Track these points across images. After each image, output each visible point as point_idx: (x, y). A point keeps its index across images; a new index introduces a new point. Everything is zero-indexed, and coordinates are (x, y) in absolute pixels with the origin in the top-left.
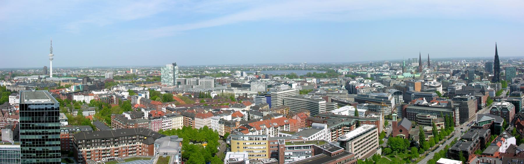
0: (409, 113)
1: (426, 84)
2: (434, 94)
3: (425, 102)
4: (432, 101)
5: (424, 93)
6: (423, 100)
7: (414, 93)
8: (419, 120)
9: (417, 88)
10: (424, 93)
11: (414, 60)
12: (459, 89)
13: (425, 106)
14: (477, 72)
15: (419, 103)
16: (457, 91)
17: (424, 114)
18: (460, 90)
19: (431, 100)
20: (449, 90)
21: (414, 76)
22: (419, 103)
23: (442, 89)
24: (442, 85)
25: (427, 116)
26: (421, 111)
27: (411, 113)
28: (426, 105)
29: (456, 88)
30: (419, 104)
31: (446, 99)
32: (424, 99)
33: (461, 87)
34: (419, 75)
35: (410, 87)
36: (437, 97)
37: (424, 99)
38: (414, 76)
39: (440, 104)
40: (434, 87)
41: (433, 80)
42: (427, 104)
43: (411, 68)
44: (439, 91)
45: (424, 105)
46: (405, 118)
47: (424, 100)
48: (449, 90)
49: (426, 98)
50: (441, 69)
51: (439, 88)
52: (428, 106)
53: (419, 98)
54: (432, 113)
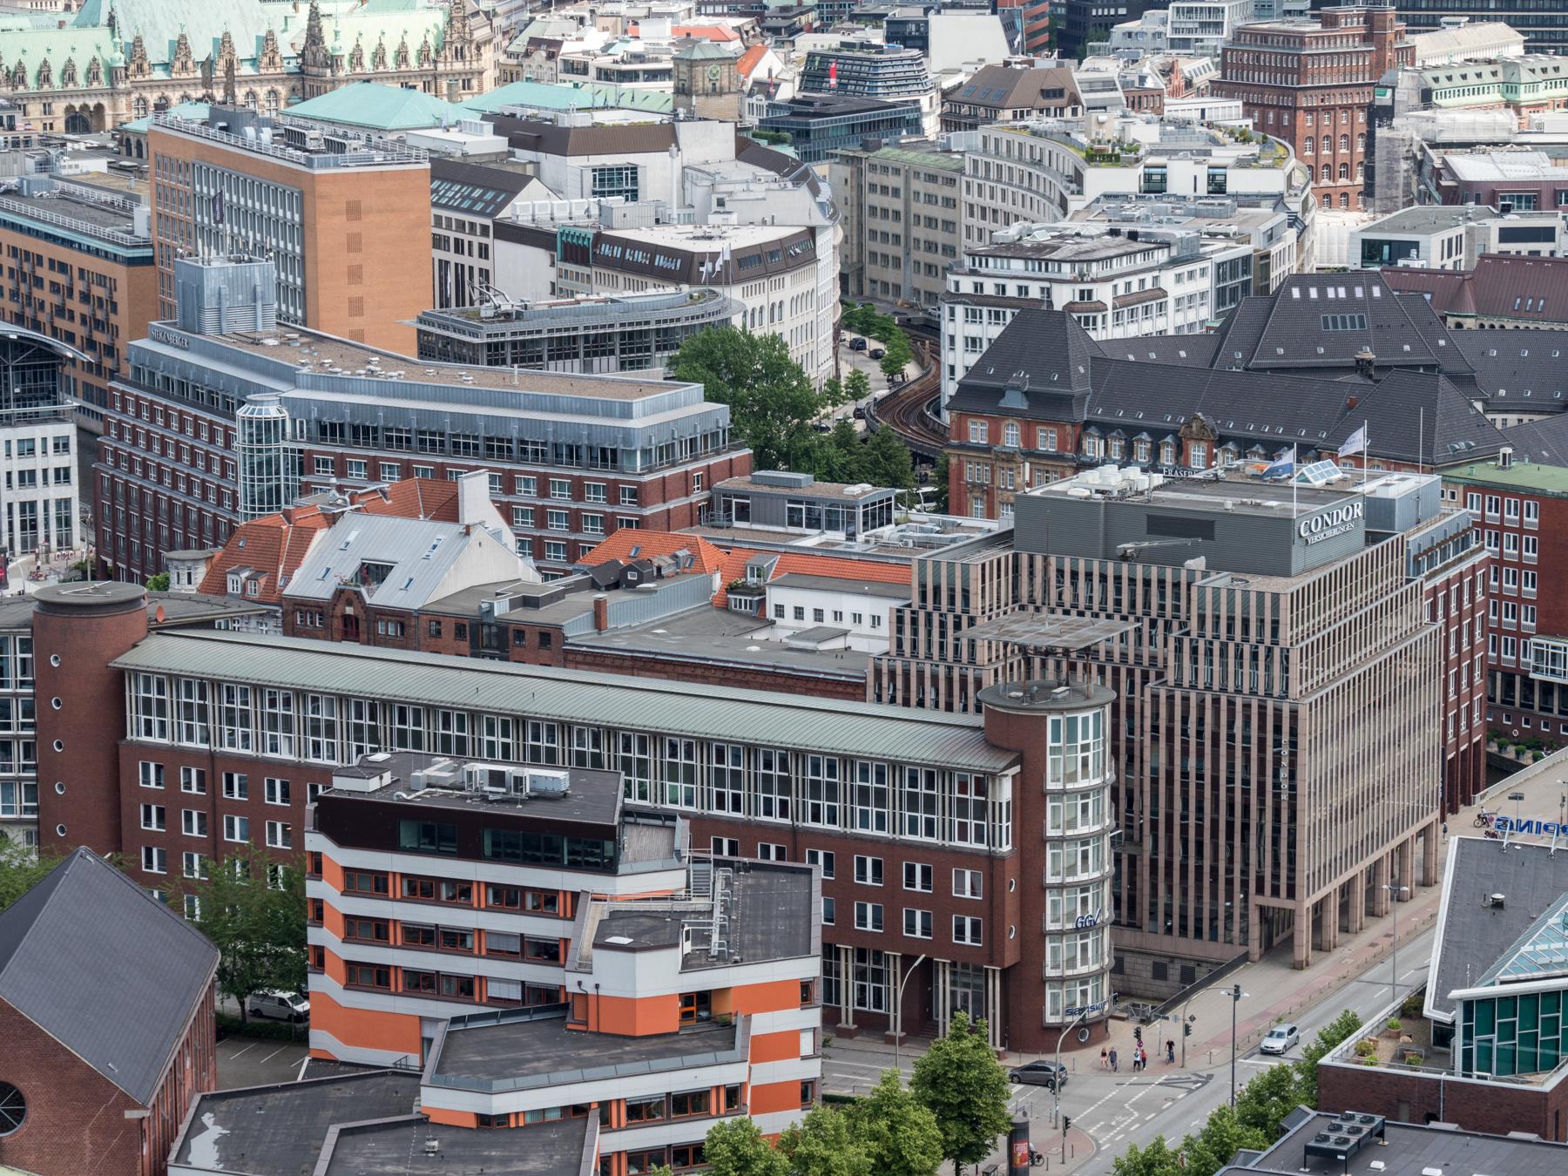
0: (170, 761)
1: (527, 207)
6: (448, 511)
7: (288, 376)
9: (355, 274)
12: (1170, 322)
15: (374, 572)
16: (1104, 361)
18: (1179, 340)
20: (973, 342)
21: (314, 36)
22: (374, 572)
23: (830, 313)
24: (829, 242)
27: (213, 767)
28: (501, 609)
29: (1103, 293)
30: (382, 596)
31: (878, 515)
32: (476, 491)
33: (1206, 284)
35: (215, 267)
36: (730, 469)
37: (476, 491)
38: (314, 36)
39: (774, 596)
40: (683, 267)
41: (662, 137)
42: (529, 602)
44: (775, 339)
45: (469, 607)
46: (87, 863)
47: (469, 514)
48: (956, 326)
49: (506, 483)
51: (790, 287)
53: (374, 470)
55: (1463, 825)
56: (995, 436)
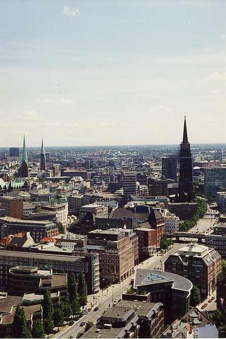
2: (48, 224)
3: (29, 242)
4: (44, 240)
5: (28, 222)
8: (13, 280)
10: (28, 222)
11: (14, 152)
13: (28, 250)
14: (142, 179)
17: (25, 268)
19: (43, 237)
21: (10, 185)
25: (32, 271)
26: (19, 261)
32: (28, 234)
34: (22, 184)
37: (28, 234)
38: (10, 185)
42: (34, 246)
43: (5, 168)
49: (31, 235)
50: (68, 170)
51: (63, 211)
52: (36, 251)
54: (42, 264)
55: (136, 268)
56: (85, 226)
